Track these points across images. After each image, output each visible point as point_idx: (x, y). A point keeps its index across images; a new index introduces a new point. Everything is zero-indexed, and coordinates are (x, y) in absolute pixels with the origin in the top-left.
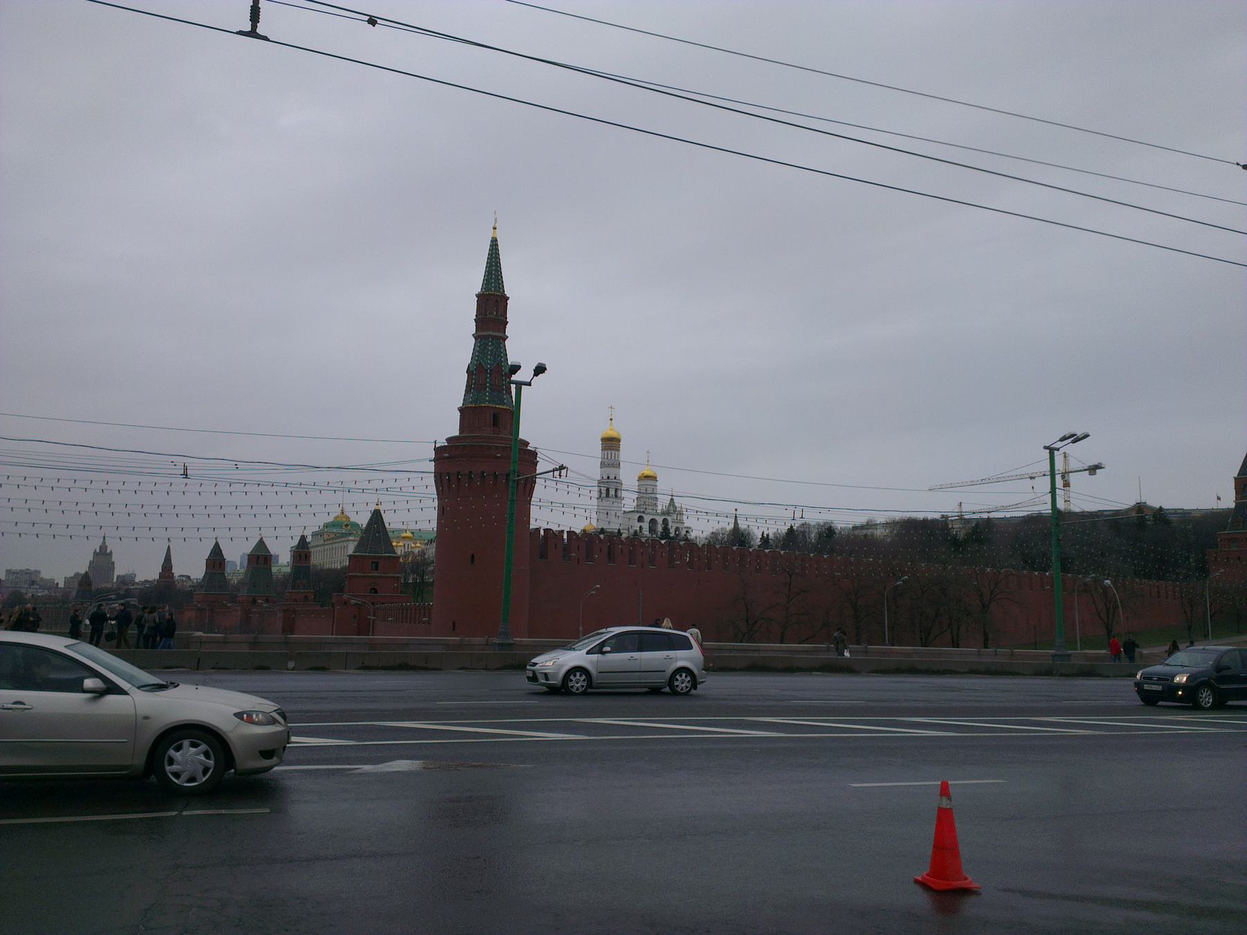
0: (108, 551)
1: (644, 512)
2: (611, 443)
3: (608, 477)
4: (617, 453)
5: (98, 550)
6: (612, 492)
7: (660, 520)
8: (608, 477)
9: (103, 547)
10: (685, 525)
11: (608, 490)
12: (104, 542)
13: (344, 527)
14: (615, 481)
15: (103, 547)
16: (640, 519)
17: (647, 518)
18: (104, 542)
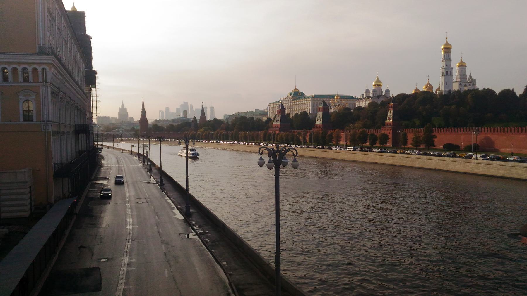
0: (125, 108)
1: (461, 82)
2: (448, 49)
3: (447, 66)
4: (449, 54)
5: (121, 108)
6: (449, 73)
7: (468, 84)
8: (447, 66)
9: (123, 106)
10: (477, 87)
11: (447, 73)
12: (123, 104)
13: (299, 94)
14: (450, 67)
15: (123, 106)
16: (460, 84)
17: (463, 84)
18: (123, 104)
